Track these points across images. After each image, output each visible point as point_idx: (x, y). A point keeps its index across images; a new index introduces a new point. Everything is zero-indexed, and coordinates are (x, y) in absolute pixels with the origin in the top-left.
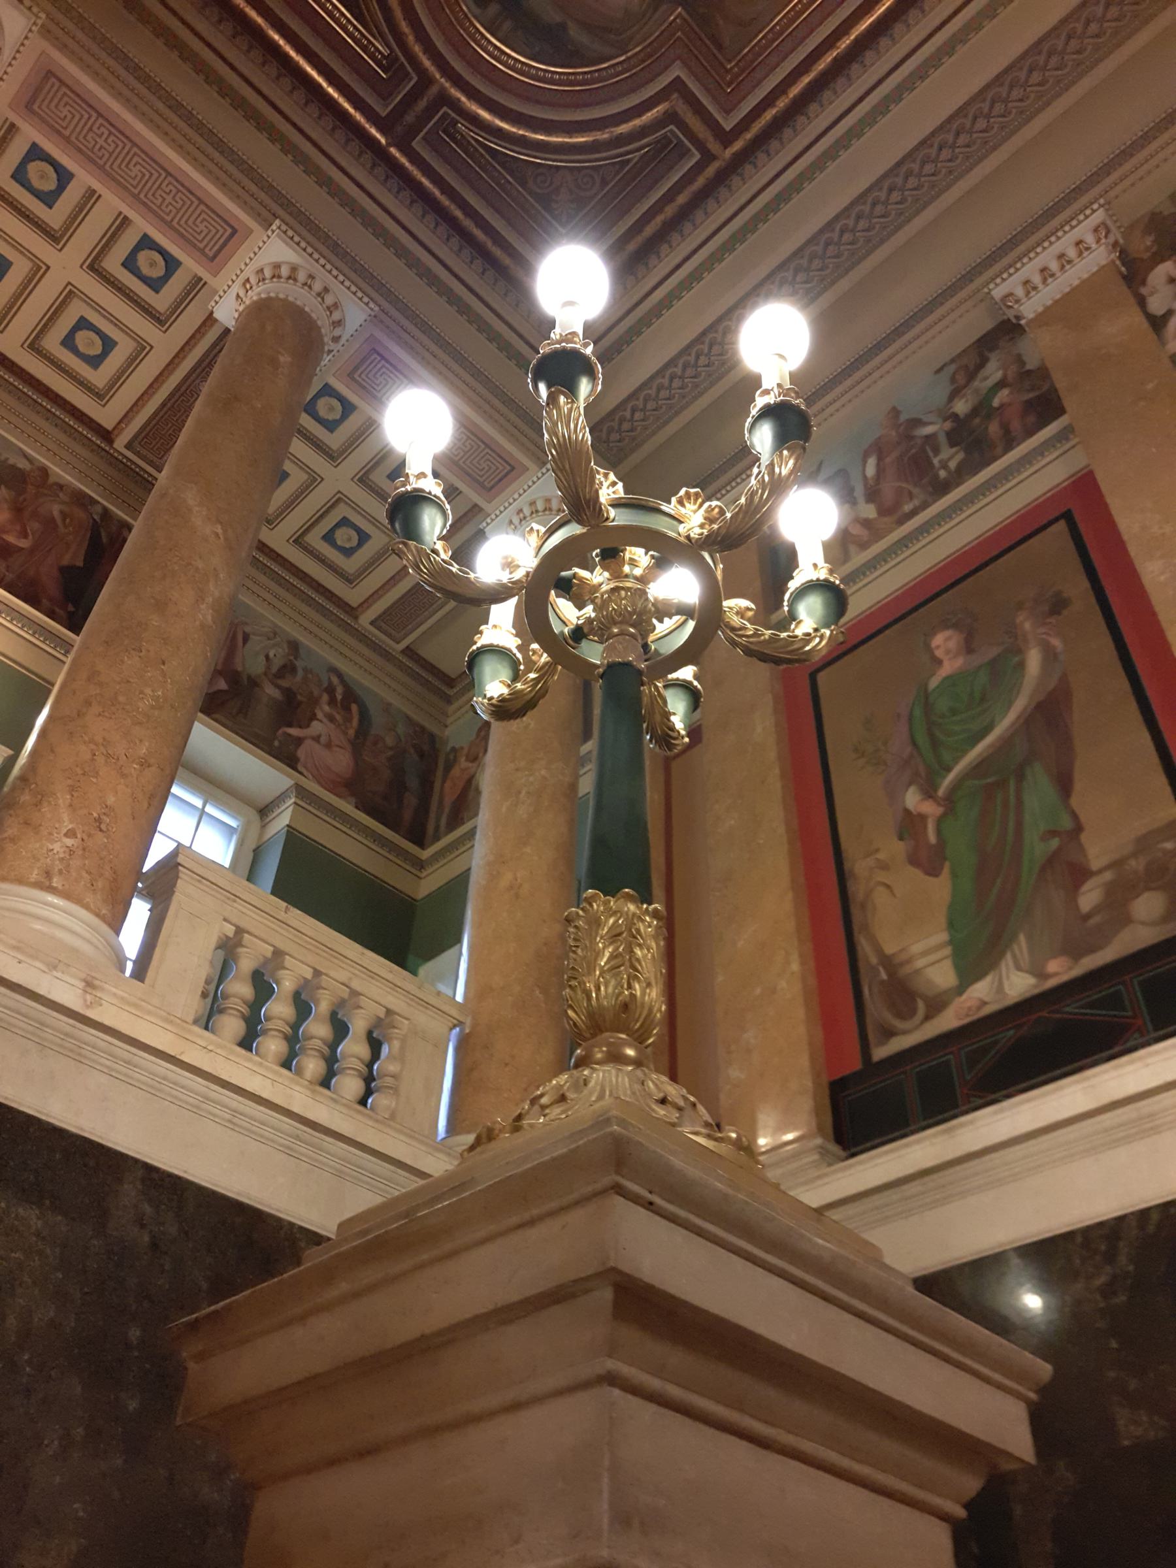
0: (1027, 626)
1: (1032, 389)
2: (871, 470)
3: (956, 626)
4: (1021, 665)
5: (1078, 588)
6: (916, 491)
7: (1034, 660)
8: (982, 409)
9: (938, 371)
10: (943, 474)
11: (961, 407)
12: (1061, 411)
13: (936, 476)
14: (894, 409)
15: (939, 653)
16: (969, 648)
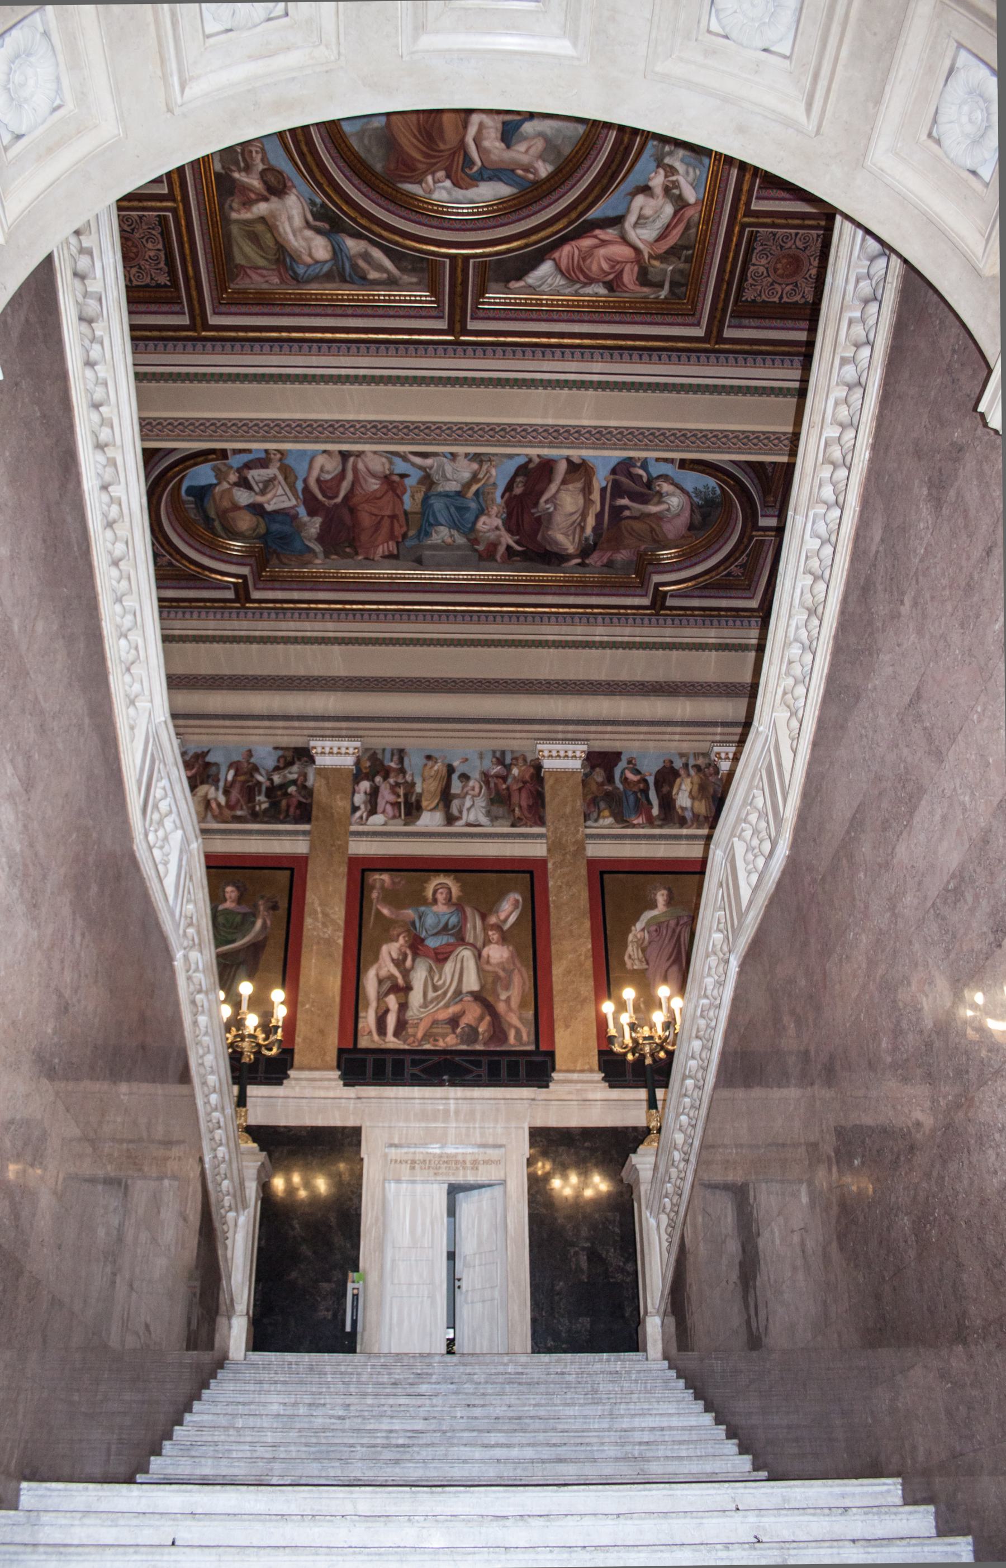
0: (262, 908)
1: (304, 797)
2: (230, 777)
3: (238, 888)
4: (253, 923)
5: (283, 904)
6: (244, 807)
7: (259, 924)
8: (284, 786)
9: (276, 748)
10: (257, 808)
11: (277, 779)
12: (308, 820)
13: (254, 807)
14: (250, 751)
15: (227, 896)
16: (239, 901)
